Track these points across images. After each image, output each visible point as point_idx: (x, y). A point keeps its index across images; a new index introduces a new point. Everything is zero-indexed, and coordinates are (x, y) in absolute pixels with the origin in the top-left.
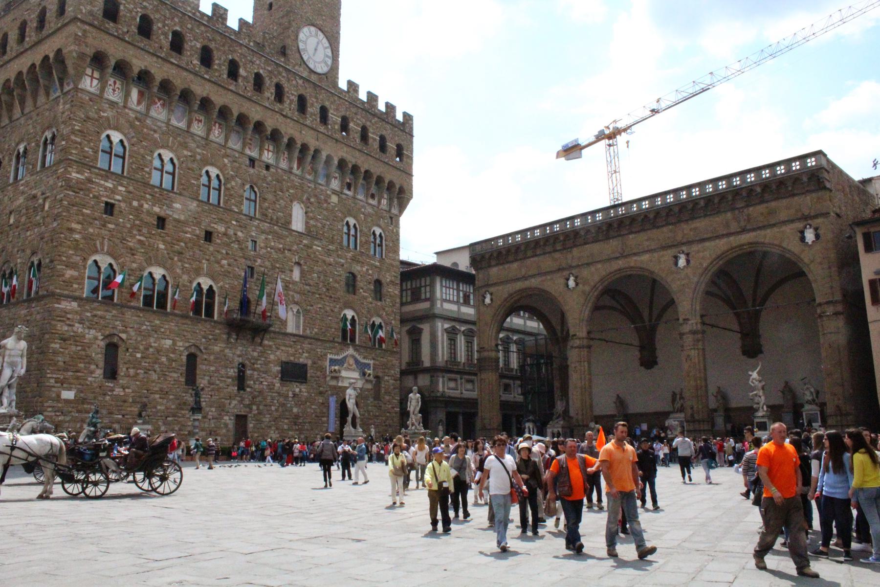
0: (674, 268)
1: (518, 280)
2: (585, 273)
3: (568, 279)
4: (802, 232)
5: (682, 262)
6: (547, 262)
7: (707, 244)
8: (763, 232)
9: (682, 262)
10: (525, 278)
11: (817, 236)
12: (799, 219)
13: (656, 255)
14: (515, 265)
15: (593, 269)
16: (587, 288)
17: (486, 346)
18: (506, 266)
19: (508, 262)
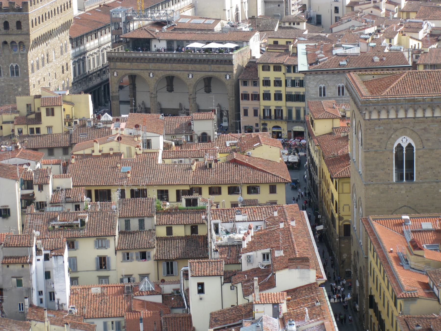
0: (188, 78)
1: (129, 69)
2: (157, 72)
3: (150, 74)
4: (226, 76)
5: (190, 77)
6: (142, 66)
7: (199, 73)
8: (215, 73)
9: (190, 77)
10: (132, 69)
11: (230, 78)
12: (226, 72)
13: (182, 72)
14: (128, 64)
15: (160, 72)
16: (157, 78)
17: (115, 91)
18: (124, 63)
19: (125, 62)
